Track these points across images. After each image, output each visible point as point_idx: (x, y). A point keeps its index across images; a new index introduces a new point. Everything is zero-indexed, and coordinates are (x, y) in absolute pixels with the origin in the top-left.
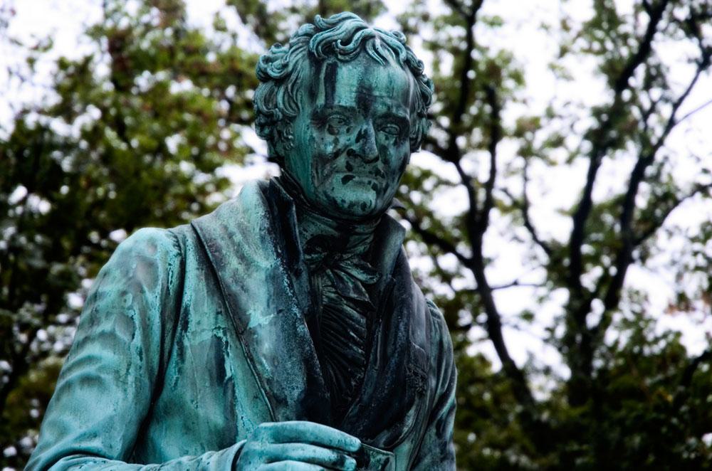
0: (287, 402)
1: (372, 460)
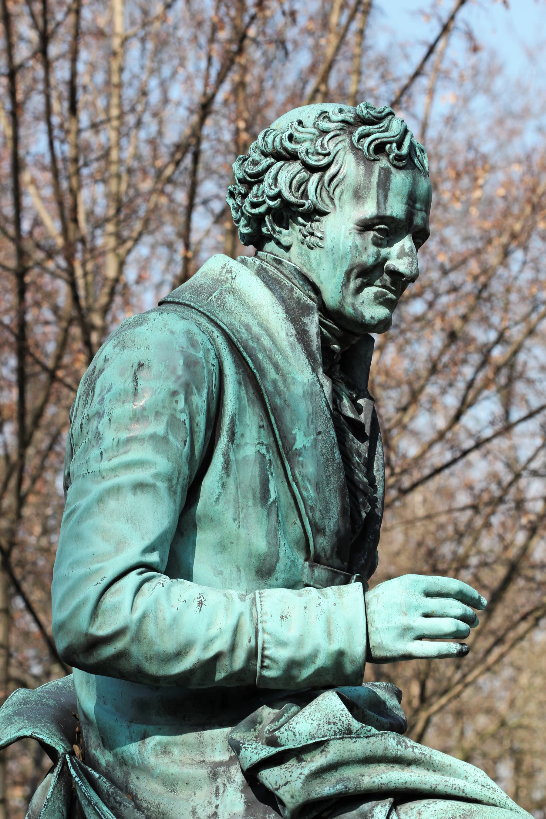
0: (325, 532)
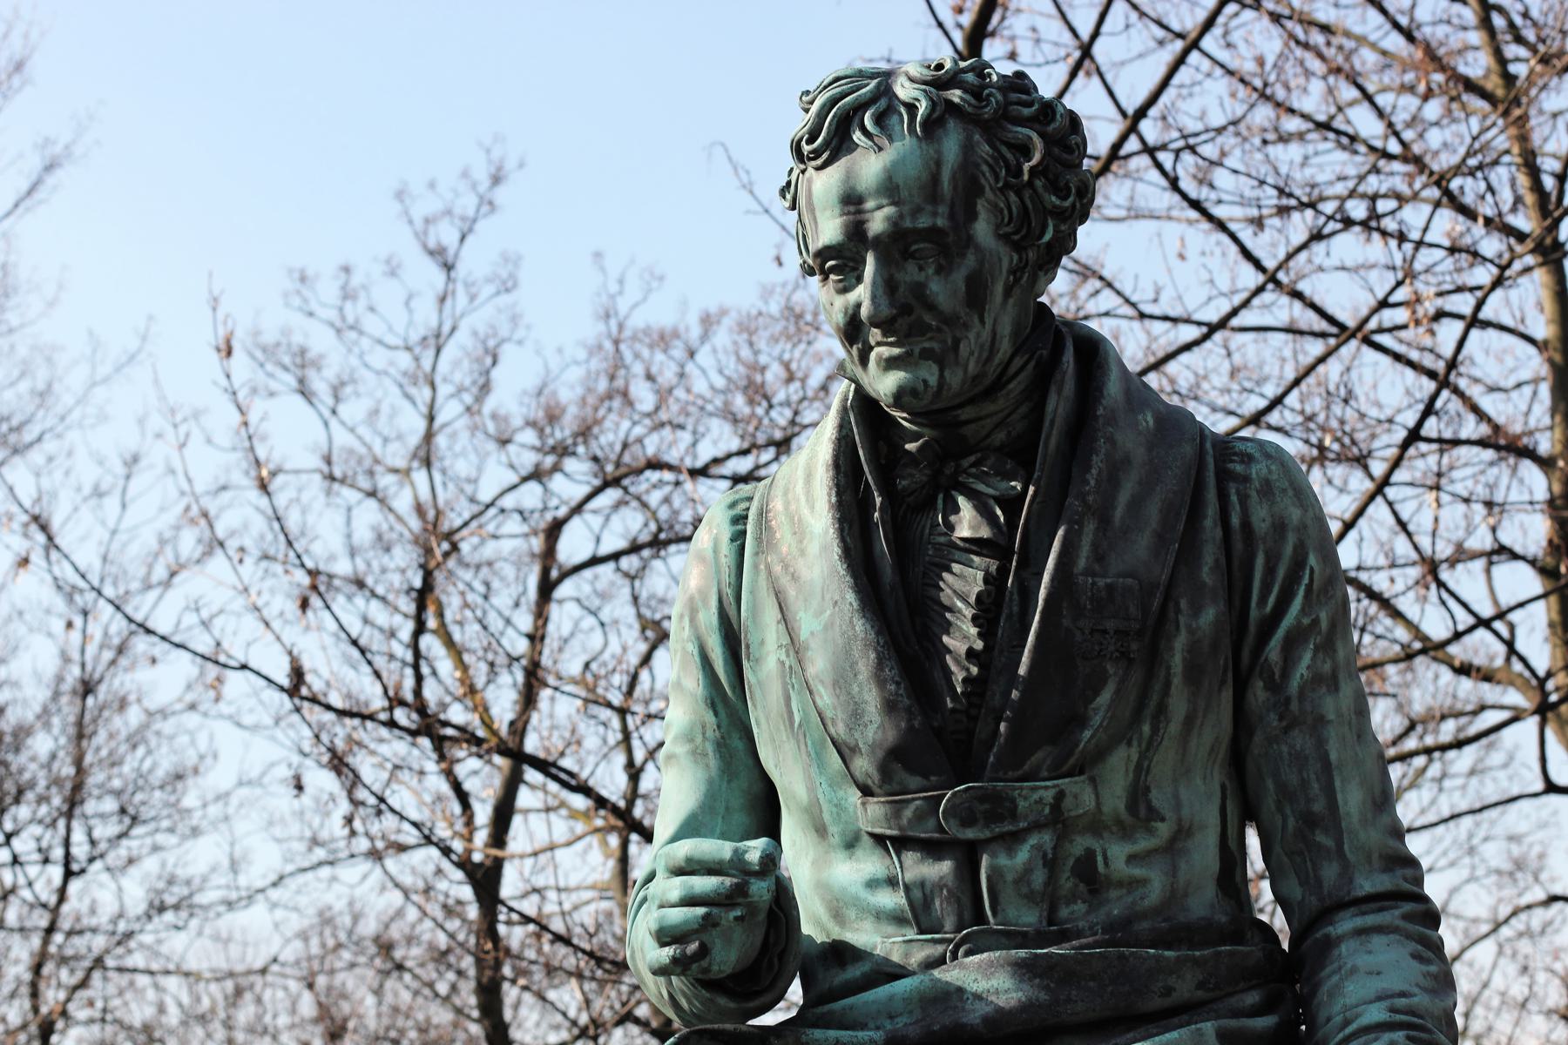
1: (1022, 804)
